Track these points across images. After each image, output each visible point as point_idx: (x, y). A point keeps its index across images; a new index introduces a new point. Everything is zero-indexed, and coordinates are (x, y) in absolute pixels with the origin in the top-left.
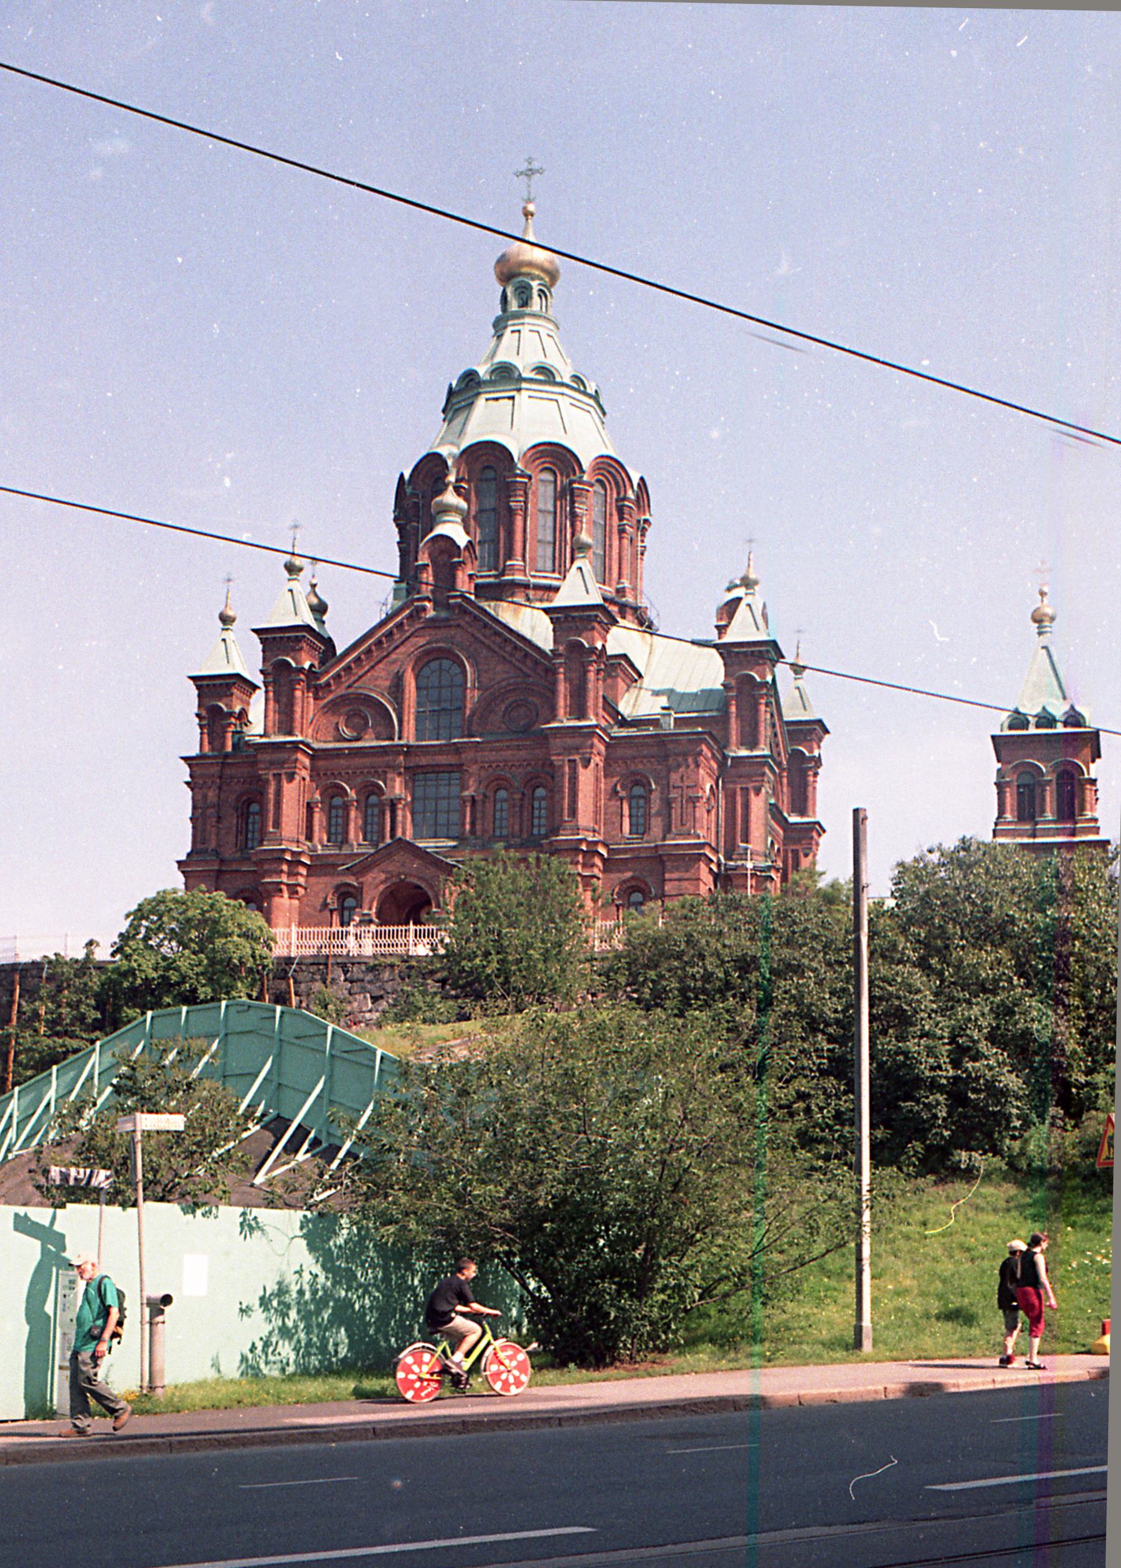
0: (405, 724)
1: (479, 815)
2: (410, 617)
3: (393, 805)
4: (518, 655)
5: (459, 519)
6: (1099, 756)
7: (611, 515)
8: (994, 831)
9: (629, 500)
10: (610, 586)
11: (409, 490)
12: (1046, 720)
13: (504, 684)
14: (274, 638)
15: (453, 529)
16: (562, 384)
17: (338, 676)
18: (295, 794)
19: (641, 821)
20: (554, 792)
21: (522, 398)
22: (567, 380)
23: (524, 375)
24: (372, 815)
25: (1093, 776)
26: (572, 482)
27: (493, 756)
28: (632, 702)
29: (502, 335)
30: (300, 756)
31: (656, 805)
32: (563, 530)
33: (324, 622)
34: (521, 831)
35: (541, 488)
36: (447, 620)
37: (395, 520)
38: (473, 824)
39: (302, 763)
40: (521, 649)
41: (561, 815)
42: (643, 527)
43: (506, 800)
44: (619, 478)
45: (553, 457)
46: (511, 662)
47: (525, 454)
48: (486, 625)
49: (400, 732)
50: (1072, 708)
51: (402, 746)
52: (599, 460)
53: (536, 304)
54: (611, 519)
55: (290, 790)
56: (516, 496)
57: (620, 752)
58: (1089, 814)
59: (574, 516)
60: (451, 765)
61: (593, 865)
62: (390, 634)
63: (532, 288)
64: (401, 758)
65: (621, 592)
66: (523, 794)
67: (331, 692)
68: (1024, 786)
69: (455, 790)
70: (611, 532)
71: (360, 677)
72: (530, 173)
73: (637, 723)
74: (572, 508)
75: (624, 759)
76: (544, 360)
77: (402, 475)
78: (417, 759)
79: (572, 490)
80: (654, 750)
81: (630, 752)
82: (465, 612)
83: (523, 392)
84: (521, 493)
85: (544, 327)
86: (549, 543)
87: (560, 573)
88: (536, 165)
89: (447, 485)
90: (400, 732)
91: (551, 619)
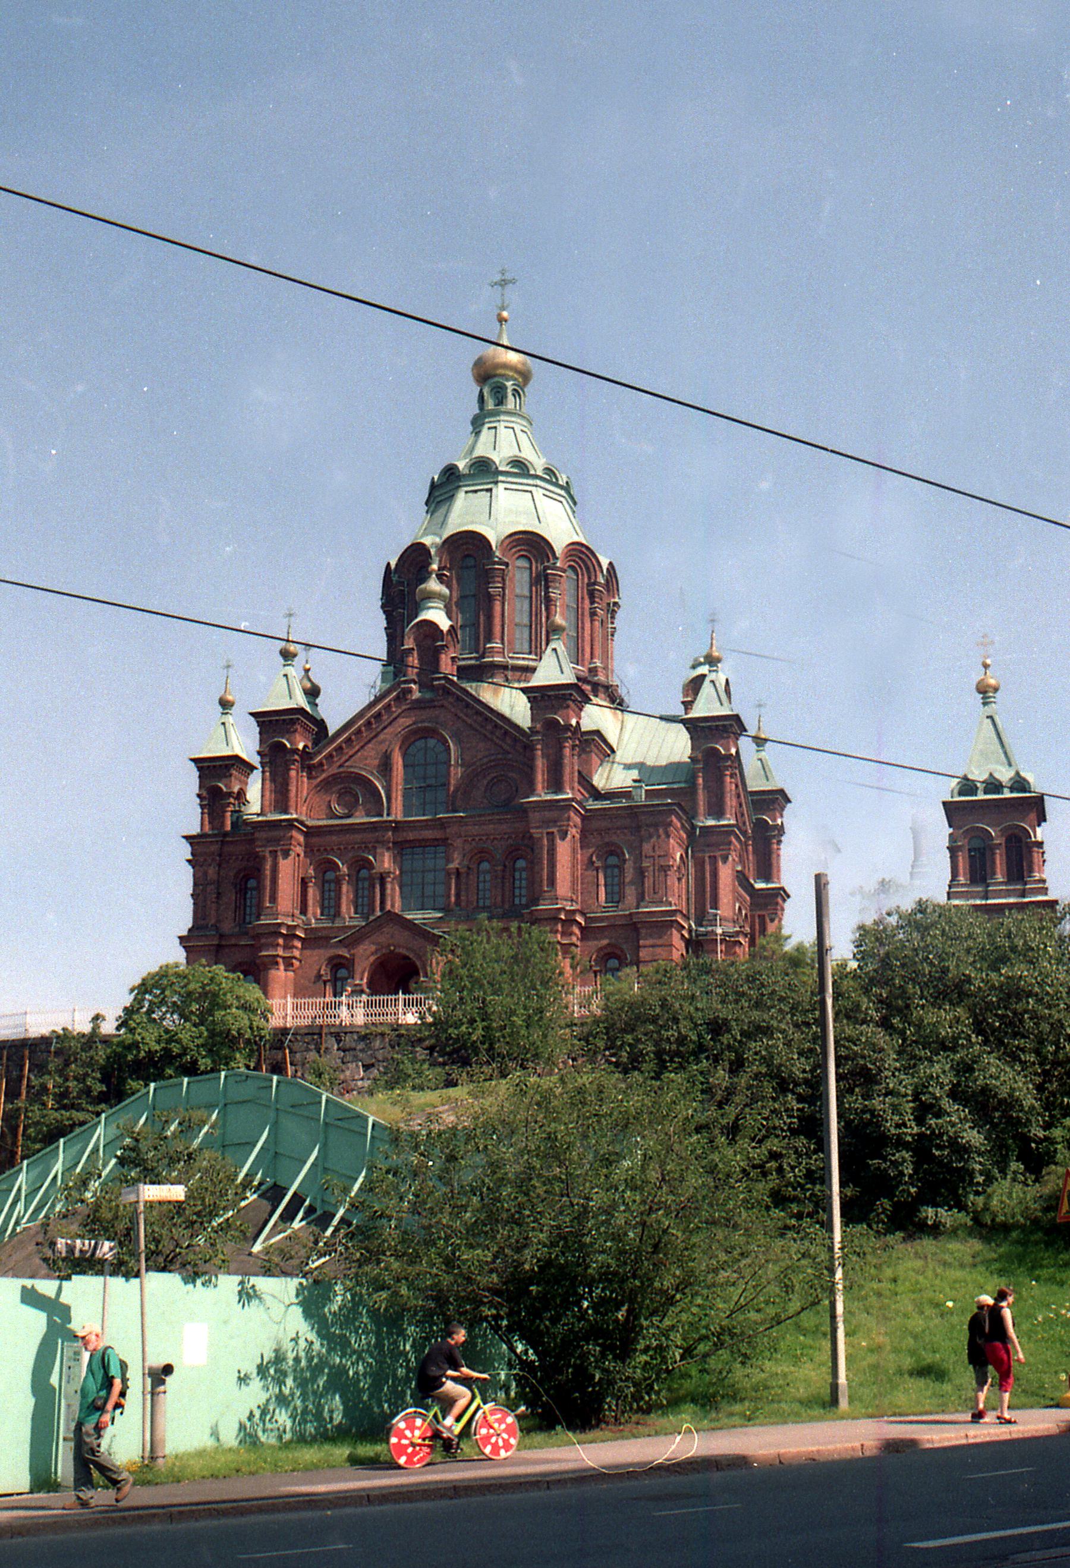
0: (393, 801)
1: (463, 887)
2: (397, 698)
3: (382, 878)
4: (498, 733)
5: (442, 606)
6: (1045, 820)
7: (583, 598)
8: (948, 893)
9: (599, 584)
10: (583, 666)
11: (395, 578)
12: (993, 785)
13: (485, 760)
14: (271, 721)
15: (437, 616)
16: (536, 477)
17: (330, 756)
18: (290, 871)
19: (616, 889)
20: (533, 864)
21: (500, 490)
22: (540, 473)
23: (500, 469)
24: (363, 888)
25: (1039, 839)
26: (546, 568)
27: (475, 830)
28: (605, 776)
29: (480, 432)
30: (294, 833)
31: (629, 874)
32: (538, 613)
33: (317, 705)
34: (503, 902)
35: (518, 576)
36: (432, 701)
37: (383, 607)
38: (458, 895)
39: (297, 840)
40: (501, 727)
41: (541, 886)
42: (612, 610)
43: (489, 872)
44: (589, 563)
45: (528, 545)
46: (492, 740)
47: (503, 541)
48: (468, 705)
49: (389, 808)
50: (1018, 773)
51: (390, 821)
52: (571, 547)
53: (511, 403)
54: (582, 603)
55: (286, 867)
56: (494, 582)
57: (595, 824)
58: (1037, 876)
59: (549, 601)
60: (436, 839)
61: (571, 934)
62: (378, 716)
63: (506, 388)
64: (390, 833)
65: (593, 671)
66: (505, 866)
67: (323, 771)
68: (975, 849)
69: (441, 863)
70: (583, 614)
71: (351, 757)
72: (503, 283)
73: (611, 795)
74: (547, 593)
75: (599, 831)
76: (519, 454)
77: (389, 564)
78: (405, 834)
79: (546, 576)
80: (627, 822)
81: (604, 824)
82: (448, 692)
83: (500, 484)
84: (500, 579)
85: (519, 424)
86: (525, 626)
87: (536, 655)
88: (508, 276)
89: (430, 573)
90: (389, 808)
91: (528, 698)
